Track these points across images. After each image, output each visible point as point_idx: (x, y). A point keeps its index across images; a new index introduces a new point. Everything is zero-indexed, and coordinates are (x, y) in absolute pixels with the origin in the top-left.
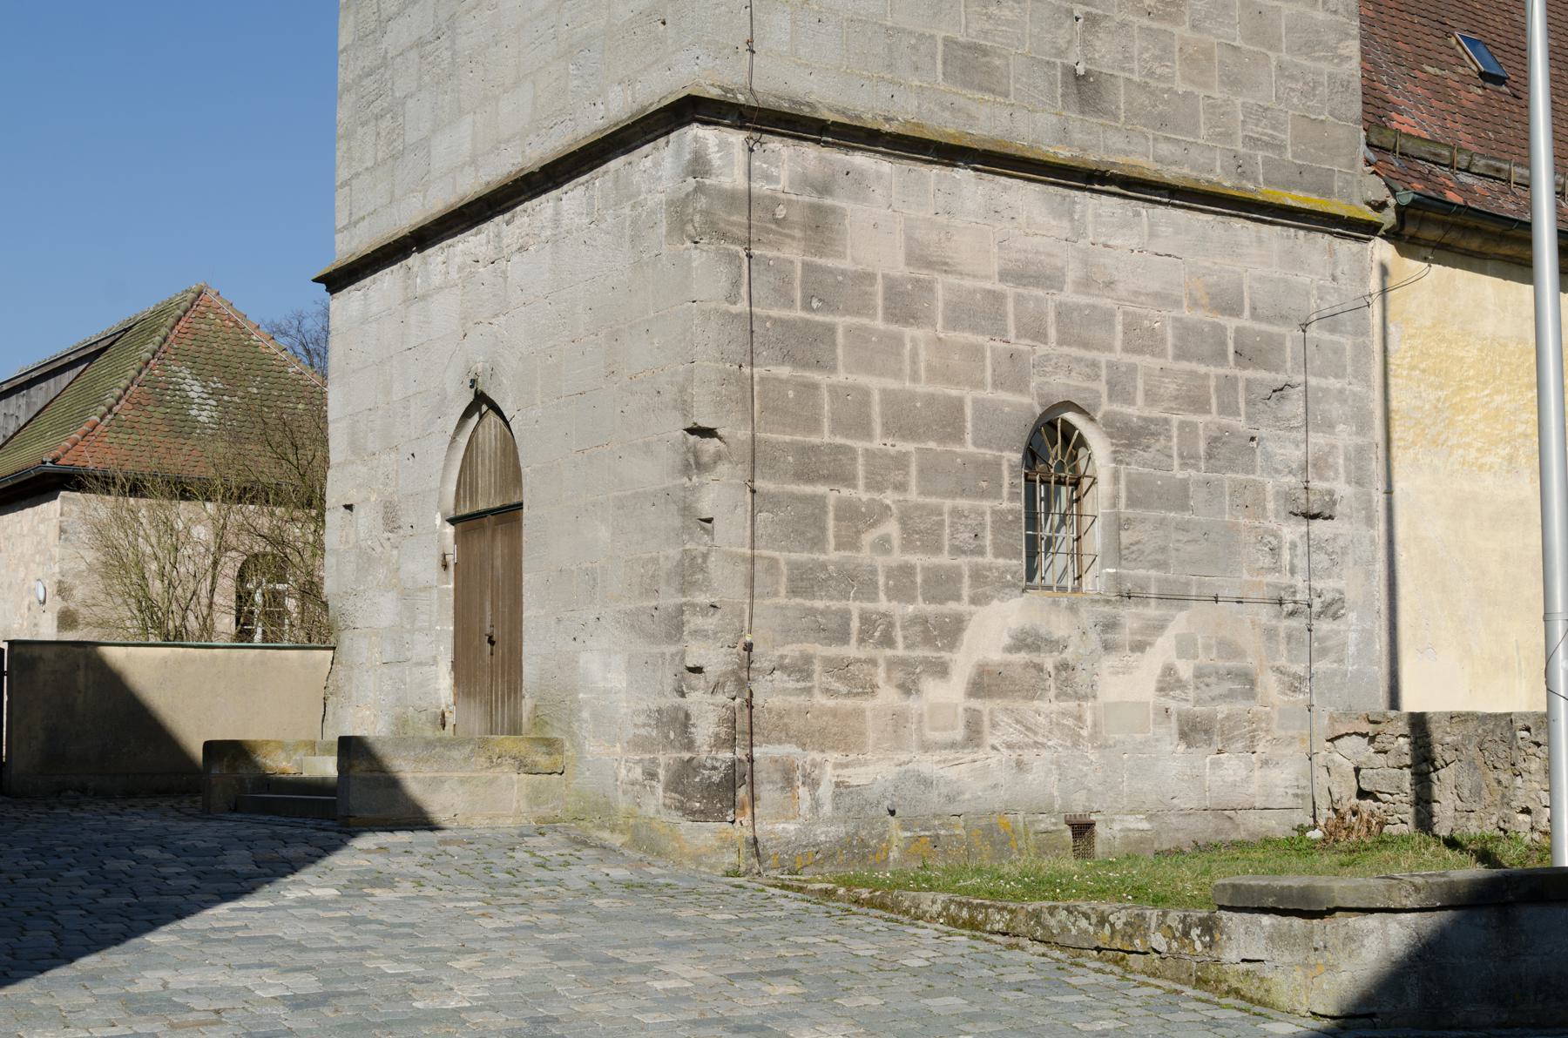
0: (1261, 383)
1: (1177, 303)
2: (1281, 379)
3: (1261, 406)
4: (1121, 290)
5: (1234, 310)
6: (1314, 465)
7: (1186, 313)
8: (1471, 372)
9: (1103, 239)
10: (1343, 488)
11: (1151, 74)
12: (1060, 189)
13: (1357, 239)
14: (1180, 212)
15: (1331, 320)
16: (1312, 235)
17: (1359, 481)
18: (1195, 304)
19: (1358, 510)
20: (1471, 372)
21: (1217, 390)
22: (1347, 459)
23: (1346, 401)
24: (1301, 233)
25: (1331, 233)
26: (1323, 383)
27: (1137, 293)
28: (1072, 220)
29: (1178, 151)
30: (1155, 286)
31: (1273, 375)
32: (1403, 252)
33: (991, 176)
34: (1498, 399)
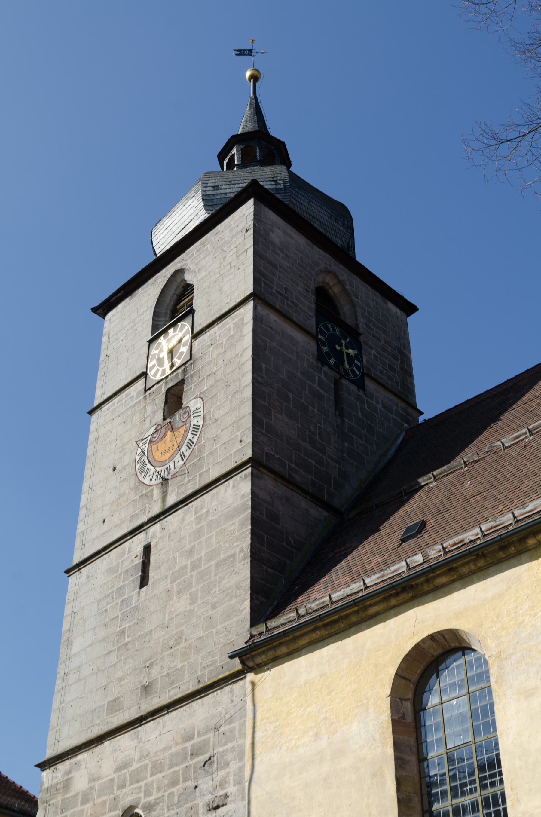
0: (199, 762)
1: (170, 748)
2: (207, 756)
3: (199, 771)
4: (152, 754)
5: (191, 738)
6: (220, 785)
7: (174, 750)
8: (294, 705)
9: (147, 739)
10: (231, 789)
11: (170, 668)
12: (135, 730)
13: (242, 679)
14: (174, 713)
15: (230, 720)
16: (224, 689)
17: (239, 782)
18: (176, 744)
19: (238, 796)
20: (294, 705)
21: (182, 774)
22: (235, 775)
23: (235, 750)
24: (219, 691)
25: (230, 684)
26: (225, 748)
27: (157, 752)
28: (138, 738)
29: (176, 690)
30: (163, 746)
31: (205, 755)
32: (256, 674)
33: (114, 739)
34: (309, 709)
